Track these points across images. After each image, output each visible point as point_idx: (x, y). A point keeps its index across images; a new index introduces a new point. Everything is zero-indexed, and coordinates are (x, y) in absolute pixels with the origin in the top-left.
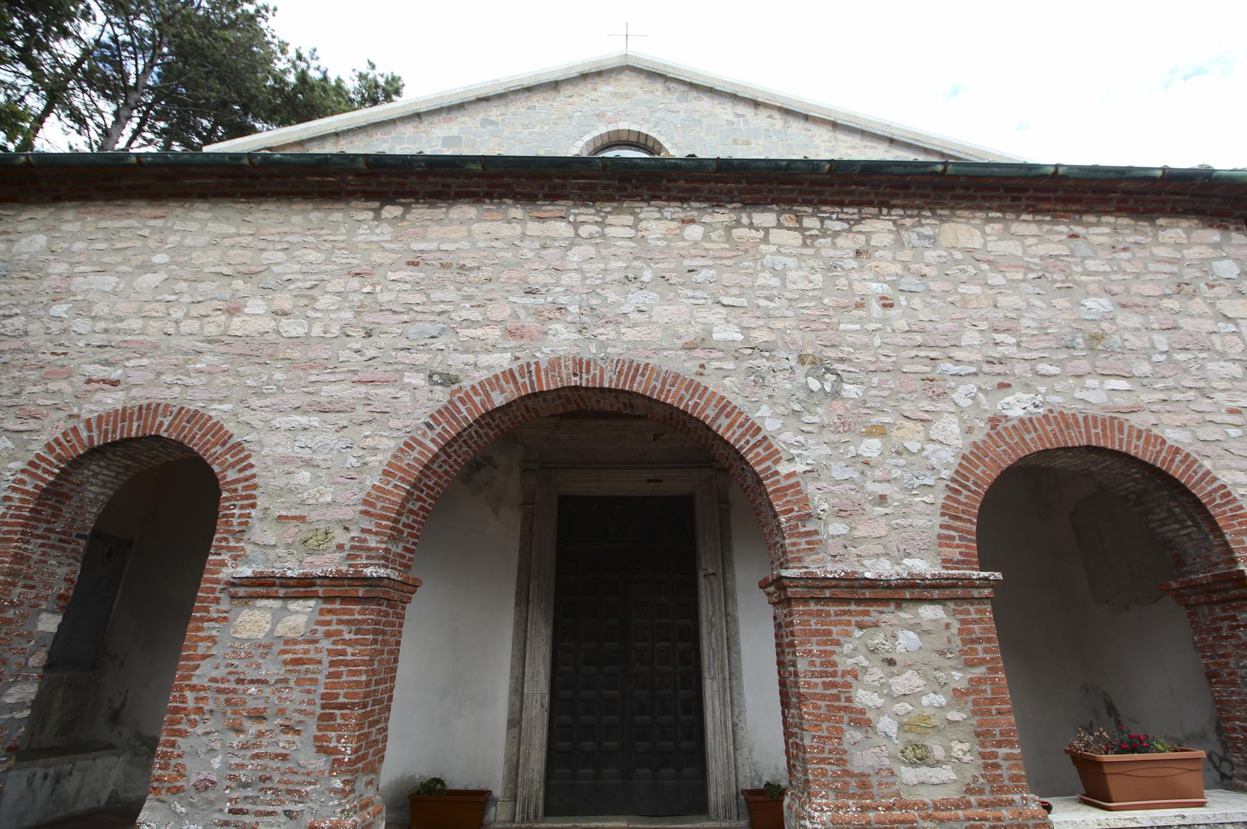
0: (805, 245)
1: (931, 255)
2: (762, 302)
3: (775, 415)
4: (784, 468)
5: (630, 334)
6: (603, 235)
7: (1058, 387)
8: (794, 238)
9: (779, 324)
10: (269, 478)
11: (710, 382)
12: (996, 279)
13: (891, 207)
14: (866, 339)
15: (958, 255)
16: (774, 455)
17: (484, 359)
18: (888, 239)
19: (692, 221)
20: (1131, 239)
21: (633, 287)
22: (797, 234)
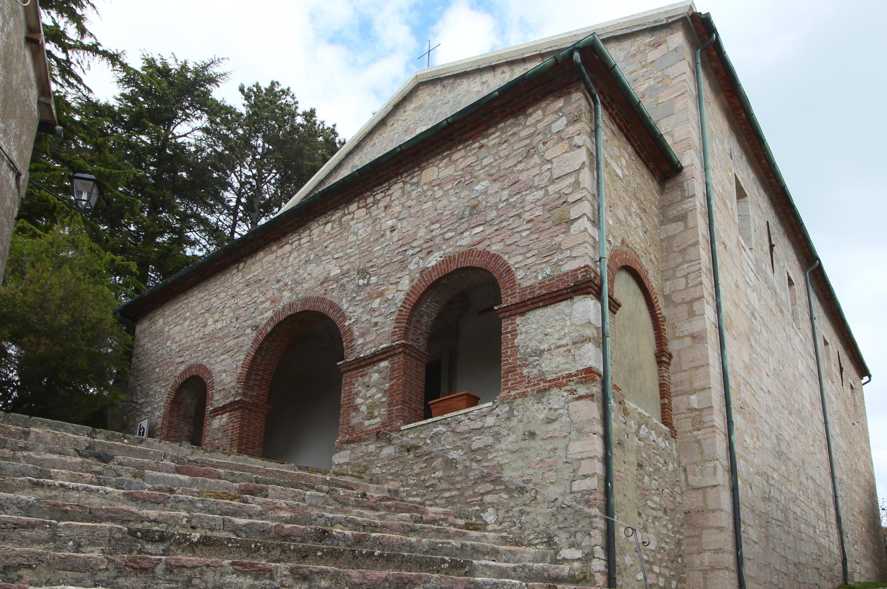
11: (328, 297)
14: (381, 252)
16: (345, 318)
18: (398, 193)
20: (510, 133)
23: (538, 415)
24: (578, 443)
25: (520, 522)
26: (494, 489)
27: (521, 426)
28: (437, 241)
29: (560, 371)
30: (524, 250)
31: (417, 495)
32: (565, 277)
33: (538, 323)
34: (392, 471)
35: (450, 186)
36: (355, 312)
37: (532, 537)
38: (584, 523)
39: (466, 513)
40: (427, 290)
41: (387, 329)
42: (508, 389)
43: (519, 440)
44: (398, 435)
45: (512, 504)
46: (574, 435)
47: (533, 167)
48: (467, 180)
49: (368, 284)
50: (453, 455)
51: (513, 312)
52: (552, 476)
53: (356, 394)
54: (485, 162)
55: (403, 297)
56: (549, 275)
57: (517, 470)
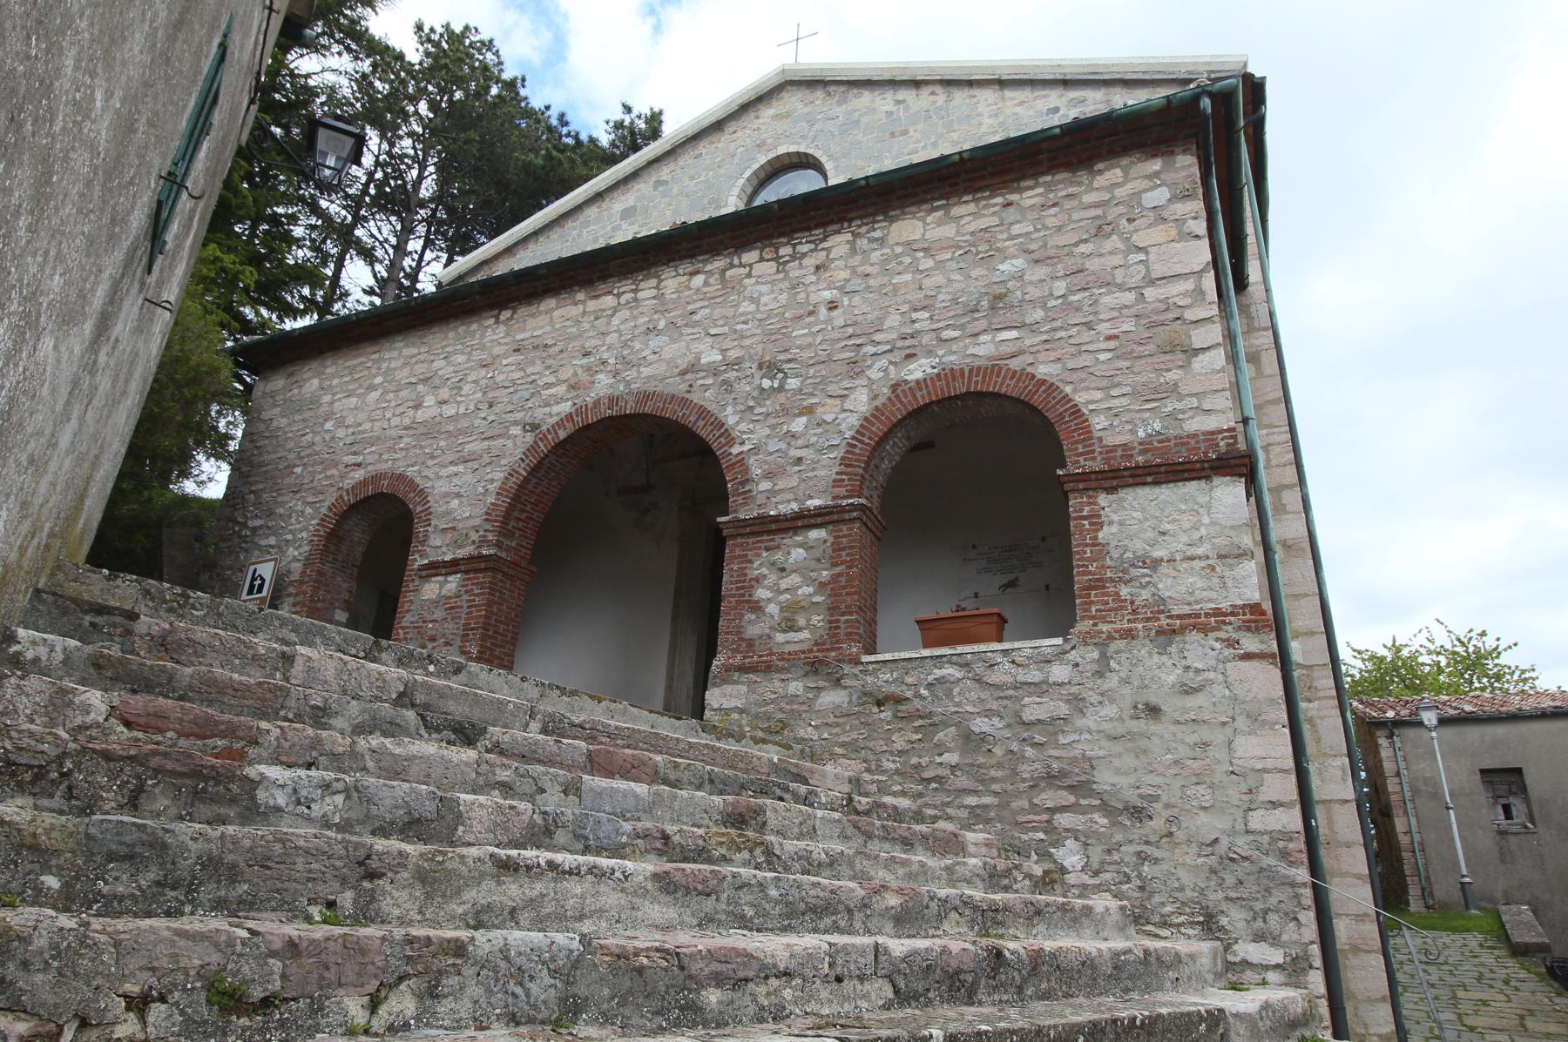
0: (778, 272)
1: (875, 256)
2: (739, 327)
3: (735, 412)
4: (735, 450)
5: (646, 371)
6: (635, 299)
7: (954, 348)
8: (770, 267)
9: (747, 342)
10: (438, 508)
11: (695, 398)
12: (927, 263)
13: (850, 221)
14: (810, 340)
15: (899, 250)
16: (731, 441)
17: (556, 409)
19: (697, 272)
20: (1064, 193)
21: (652, 336)
22: (773, 264)
23: (1163, 676)
24: (1253, 740)
25: (1139, 876)
26: (1076, 804)
27: (1126, 690)
28: (925, 339)
29: (1197, 602)
30: (1105, 383)
31: (903, 794)
32: (1193, 442)
33: (1143, 510)
34: (844, 738)
35: (949, 256)
36: (751, 432)
37: (1168, 909)
38: (1278, 895)
39: (1017, 842)
40: (904, 418)
41: (823, 473)
42: (1092, 618)
43: (1126, 717)
44: (856, 670)
45: (1119, 837)
46: (1241, 722)
47: (1110, 253)
48: (983, 250)
49: (781, 389)
50: (980, 725)
51: (1094, 485)
52: (1203, 794)
53: (757, 580)
54: (1016, 229)
55: (857, 423)
56: (1159, 433)
57: (1126, 774)
